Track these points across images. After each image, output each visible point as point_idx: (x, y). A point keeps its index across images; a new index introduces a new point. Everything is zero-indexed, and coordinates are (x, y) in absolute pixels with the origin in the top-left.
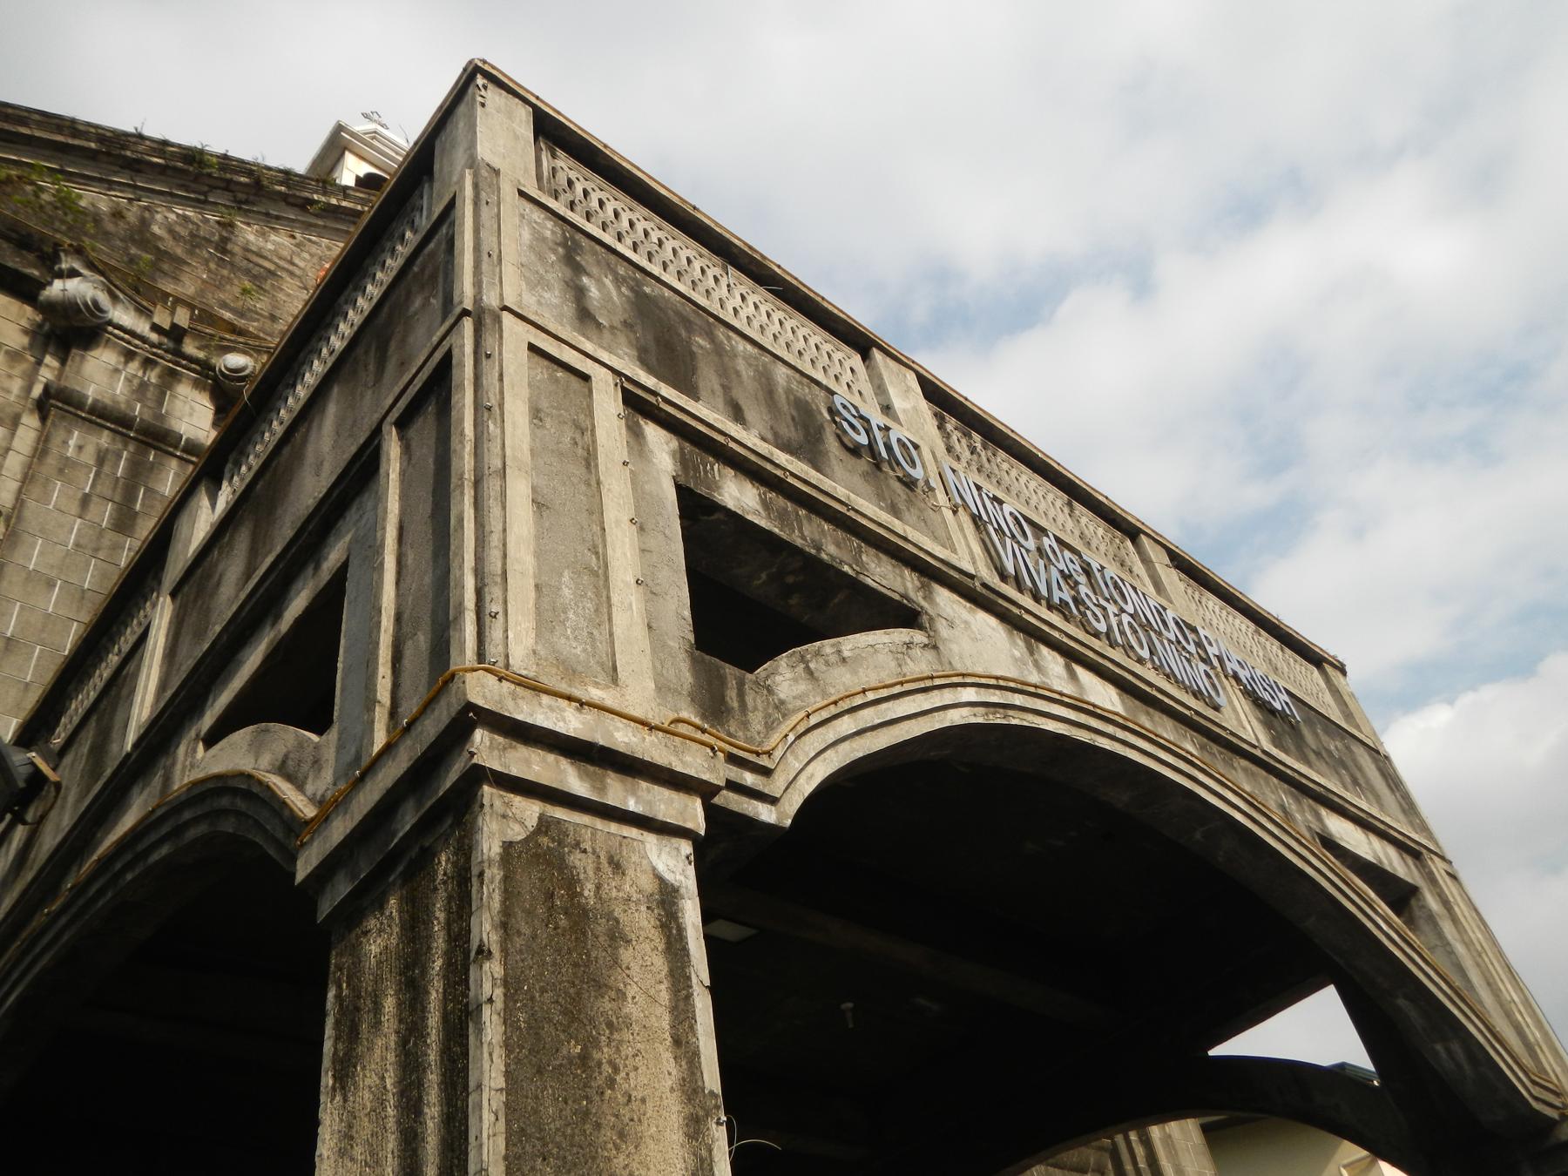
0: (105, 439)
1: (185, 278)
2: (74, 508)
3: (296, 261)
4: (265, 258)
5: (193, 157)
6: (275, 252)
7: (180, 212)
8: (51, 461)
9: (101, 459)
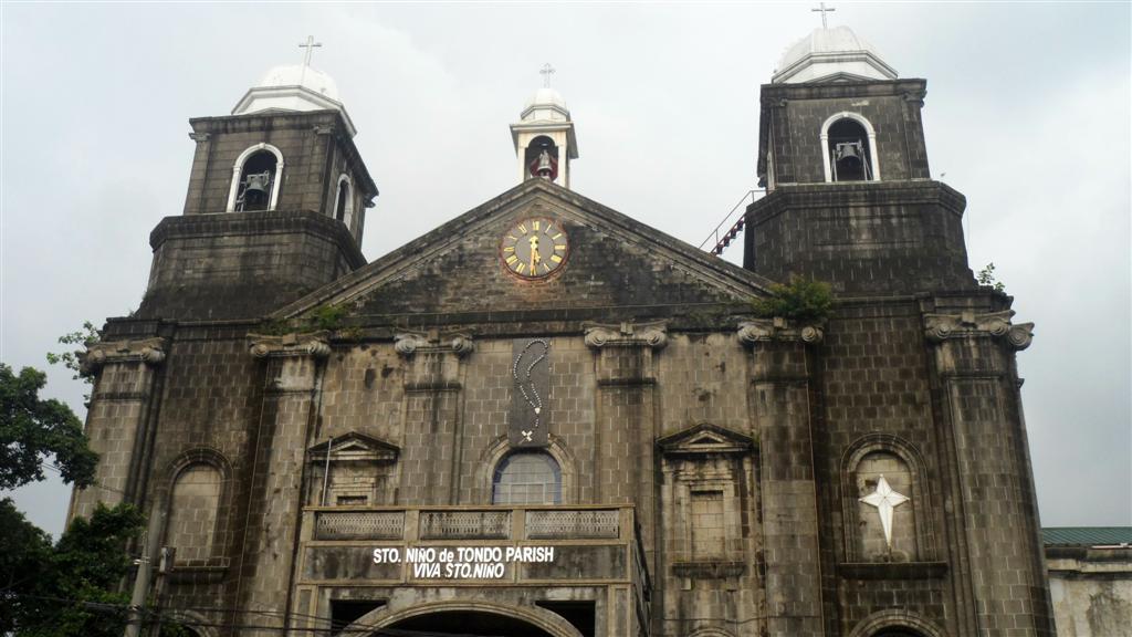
0: (424, 398)
1: (449, 291)
2: (419, 429)
3: (493, 245)
4: (479, 254)
5: (435, 233)
6: (482, 248)
7: (442, 255)
8: (411, 415)
9: (424, 407)
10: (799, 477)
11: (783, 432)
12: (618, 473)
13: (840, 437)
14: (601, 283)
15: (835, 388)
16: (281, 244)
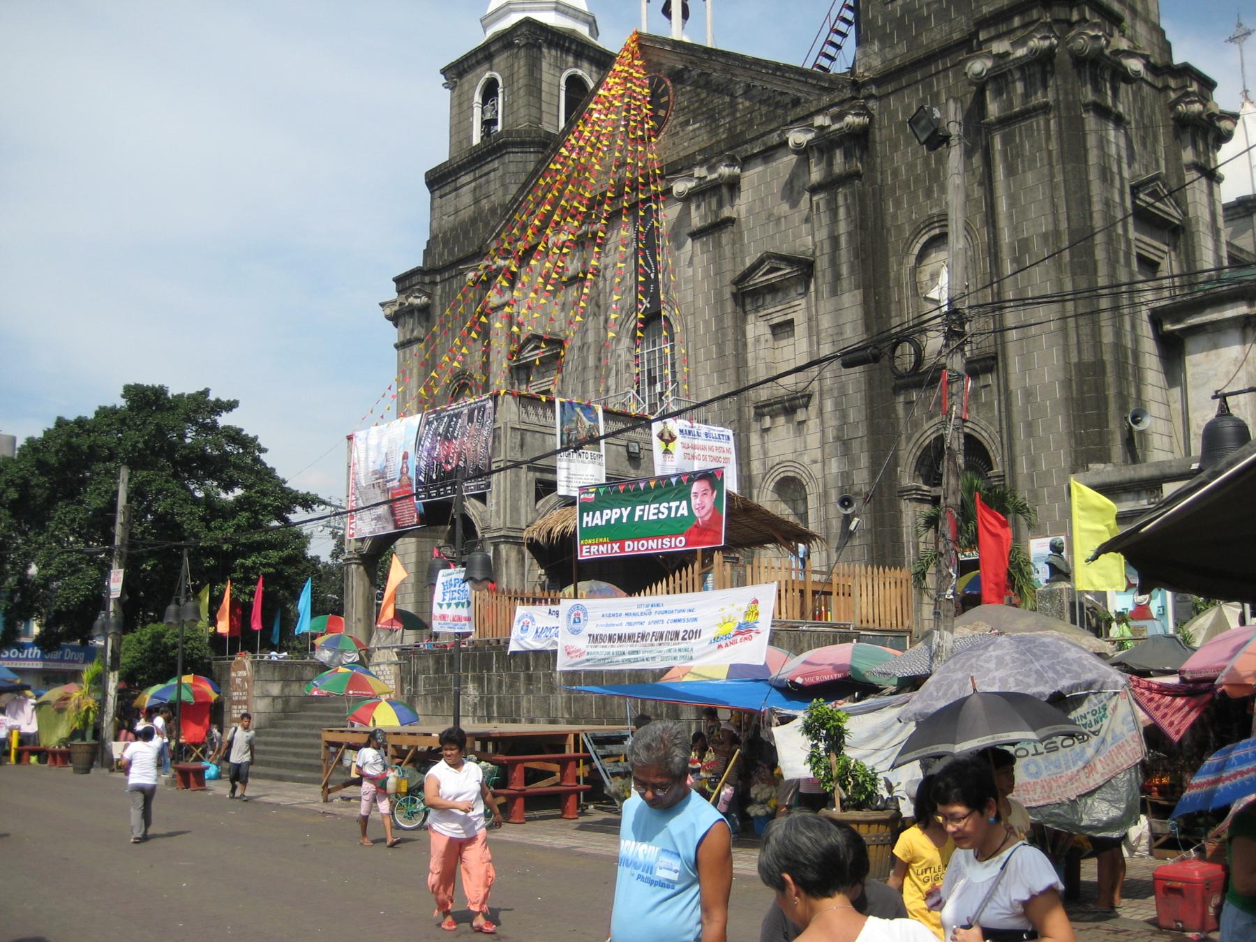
10: (850, 291)
11: (834, 239)
12: (705, 321)
13: (899, 228)
14: (698, 125)
15: (895, 173)
16: (494, 170)
